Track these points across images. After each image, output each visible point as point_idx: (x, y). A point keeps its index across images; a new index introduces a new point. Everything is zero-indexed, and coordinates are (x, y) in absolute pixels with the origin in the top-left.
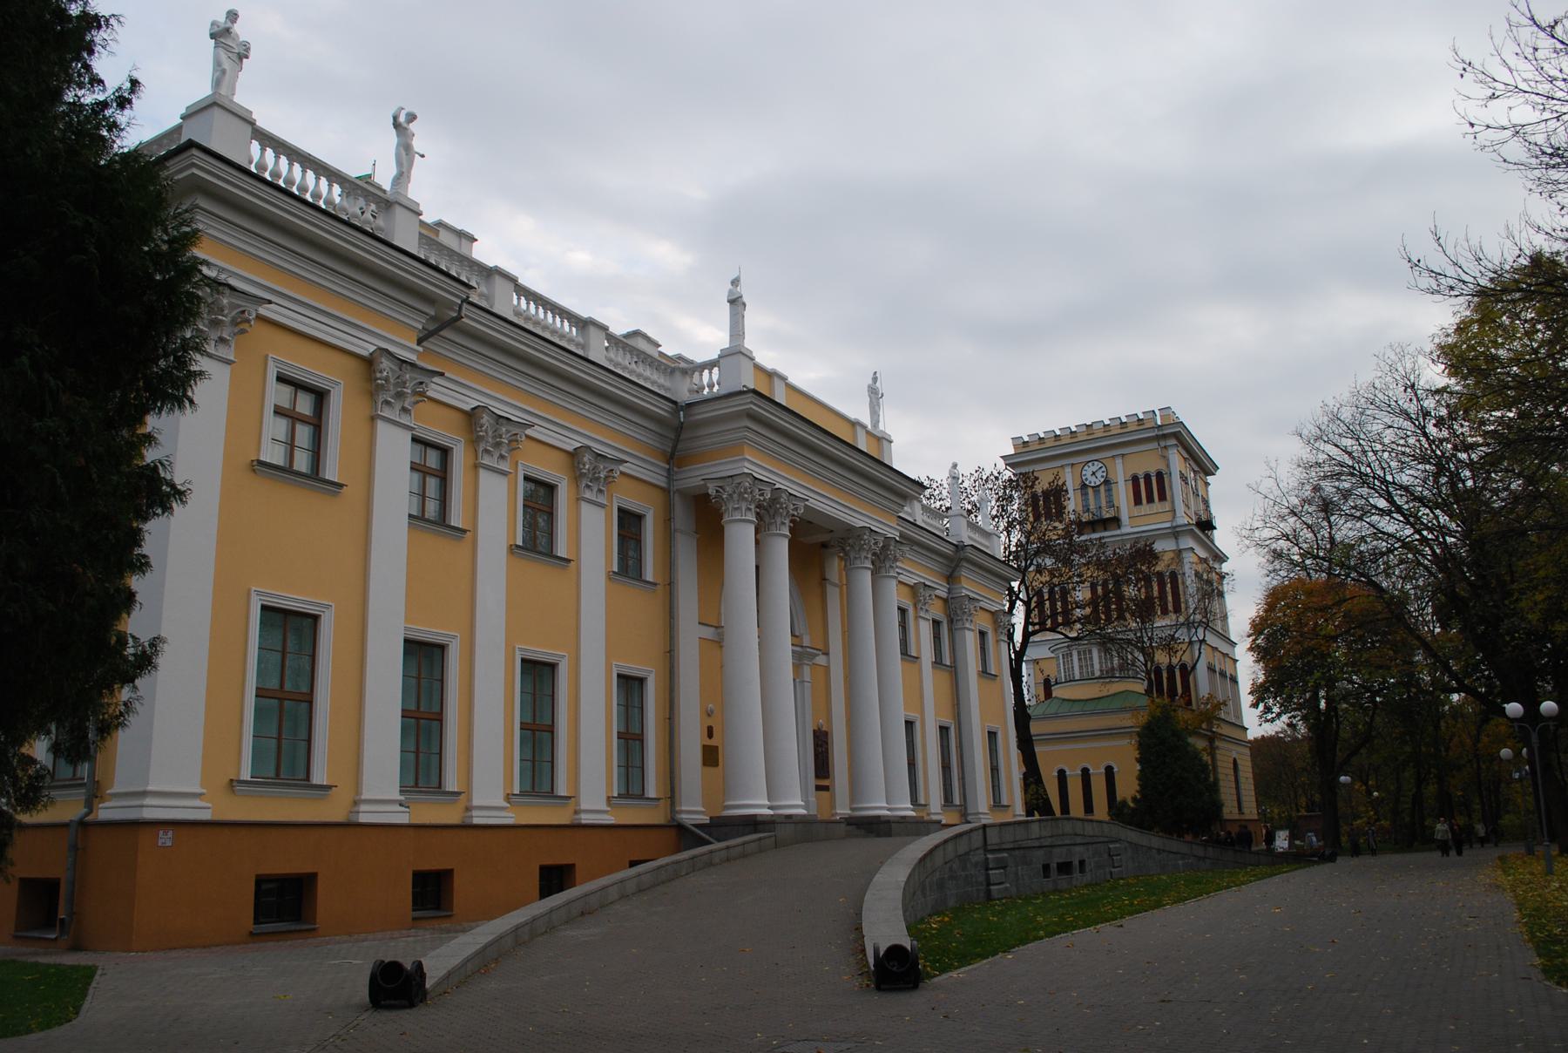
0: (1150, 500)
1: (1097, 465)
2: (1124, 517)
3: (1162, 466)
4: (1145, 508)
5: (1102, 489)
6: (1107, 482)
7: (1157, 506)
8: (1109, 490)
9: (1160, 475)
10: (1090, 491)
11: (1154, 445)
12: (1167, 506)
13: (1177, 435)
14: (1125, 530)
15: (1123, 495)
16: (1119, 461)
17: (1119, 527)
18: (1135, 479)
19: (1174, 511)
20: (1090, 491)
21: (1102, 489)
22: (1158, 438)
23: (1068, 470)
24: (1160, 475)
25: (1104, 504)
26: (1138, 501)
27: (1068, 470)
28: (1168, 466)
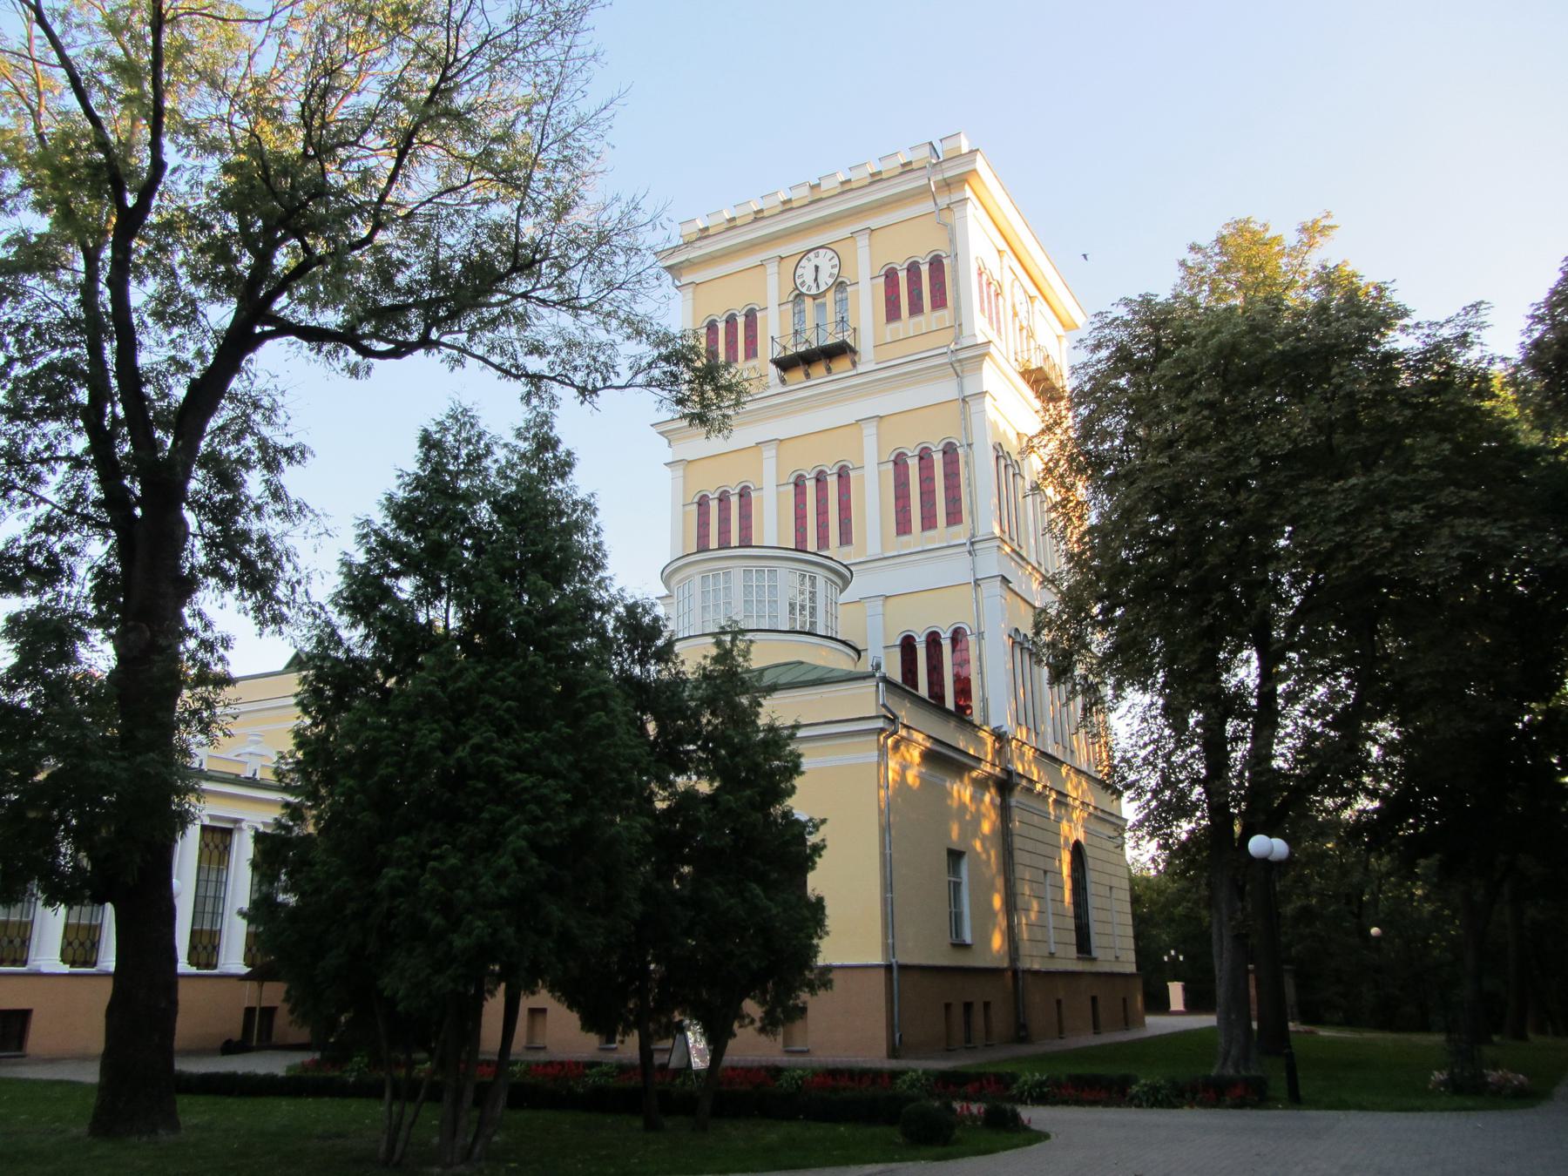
0: (916, 308)
1: (825, 261)
2: (865, 345)
4: (907, 324)
6: (840, 286)
7: (930, 318)
8: (842, 302)
10: (809, 302)
11: (927, 206)
12: (945, 315)
14: (860, 369)
15: (867, 302)
16: (863, 241)
17: (854, 364)
18: (891, 277)
20: (809, 302)
23: (772, 269)
24: (936, 264)
25: (831, 315)
26: (893, 313)
27: (772, 269)
28: (952, 241)
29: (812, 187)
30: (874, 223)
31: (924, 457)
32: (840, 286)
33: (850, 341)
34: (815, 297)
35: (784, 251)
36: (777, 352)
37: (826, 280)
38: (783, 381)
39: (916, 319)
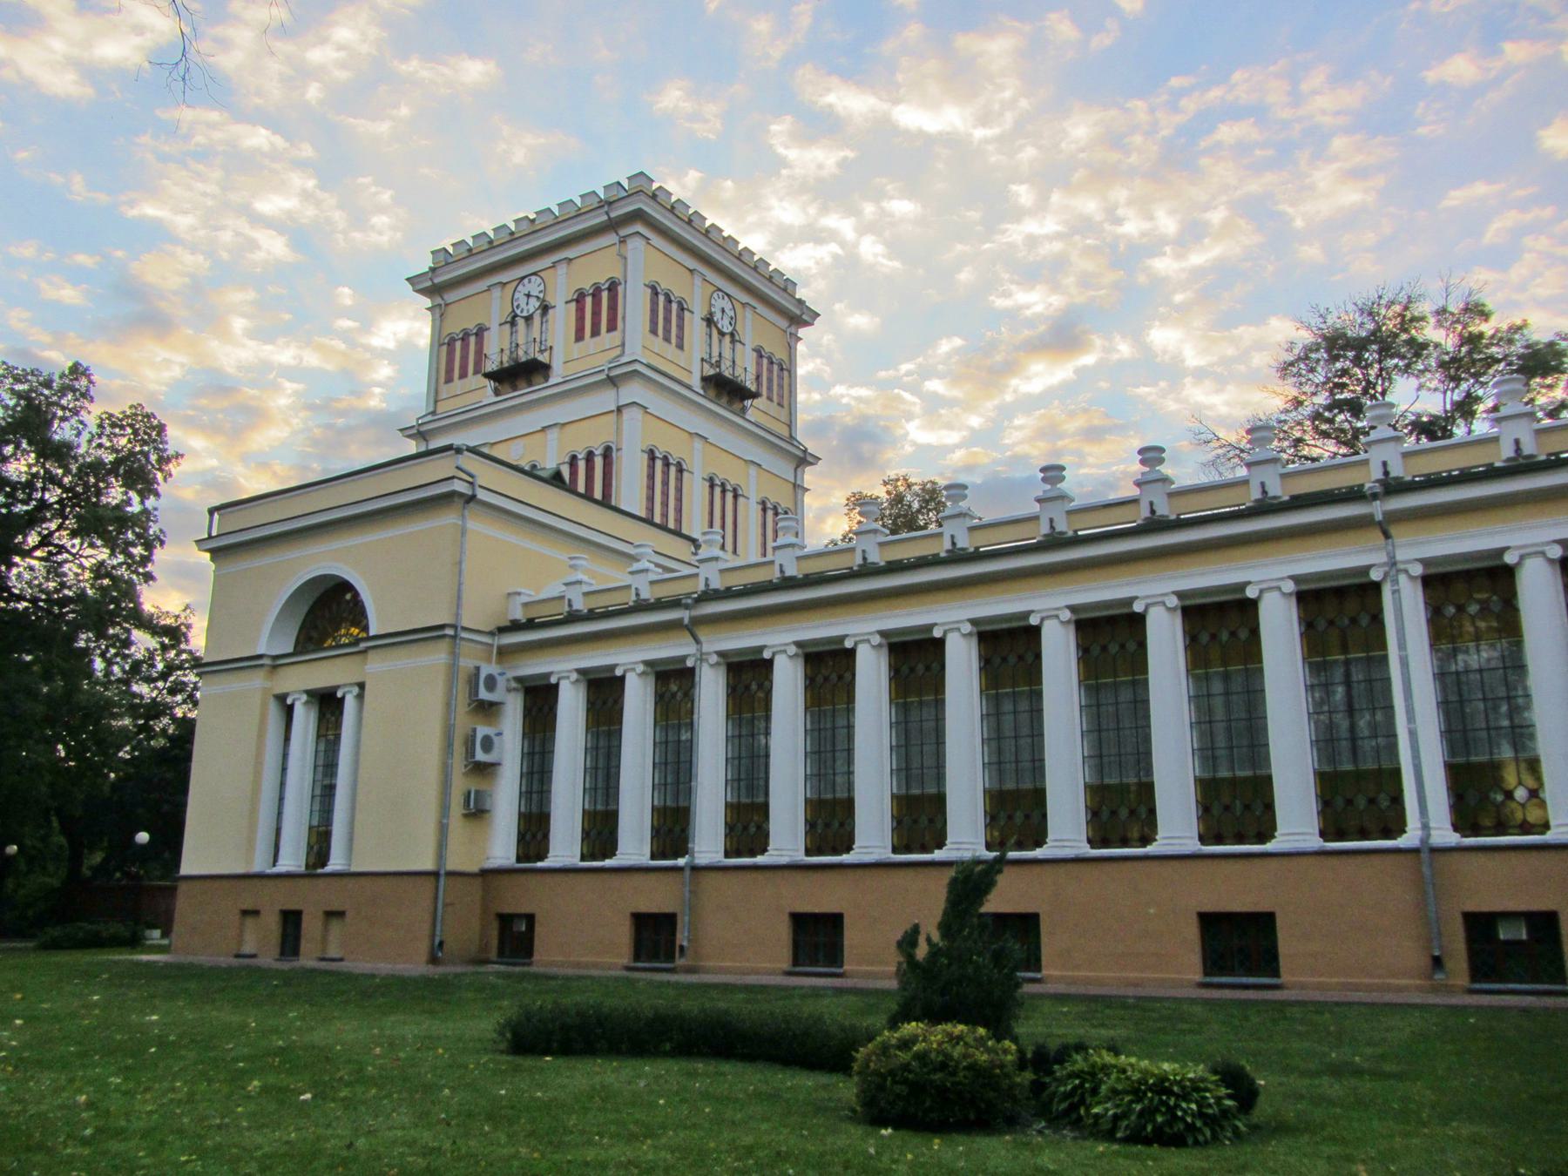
1: (534, 286)
3: (618, 275)
5: (537, 318)
9: (613, 287)
10: (521, 322)
11: (611, 238)
13: (638, 216)
14: (552, 381)
16: (562, 269)
19: (623, 345)
21: (537, 318)
22: (612, 226)
27: (497, 292)
29: (533, 221)
30: (570, 253)
31: (590, 457)
32: (545, 308)
33: (543, 358)
34: (529, 319)
35: (504, 277)
36: (491, 366)
37: (534, 303)
38: (497, 393)
39: (596, 339)
